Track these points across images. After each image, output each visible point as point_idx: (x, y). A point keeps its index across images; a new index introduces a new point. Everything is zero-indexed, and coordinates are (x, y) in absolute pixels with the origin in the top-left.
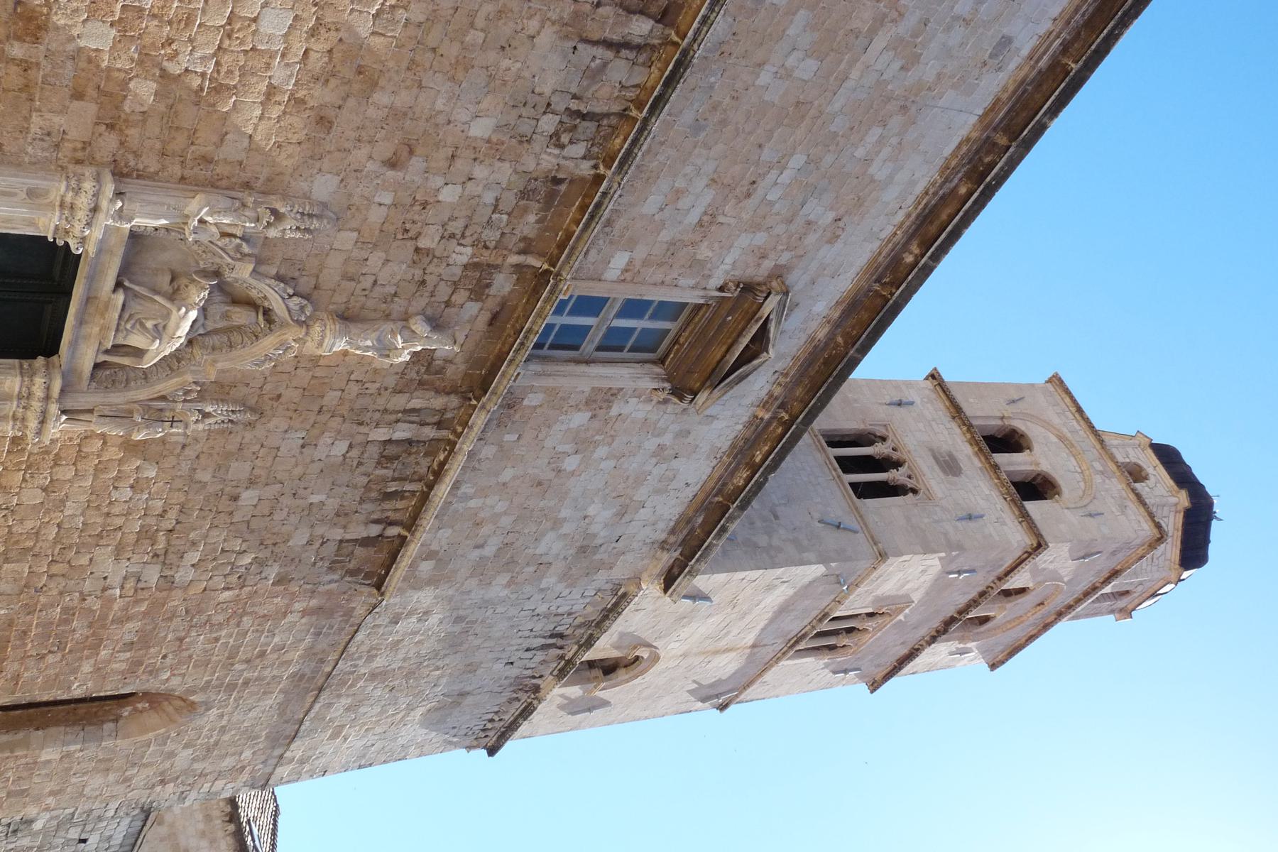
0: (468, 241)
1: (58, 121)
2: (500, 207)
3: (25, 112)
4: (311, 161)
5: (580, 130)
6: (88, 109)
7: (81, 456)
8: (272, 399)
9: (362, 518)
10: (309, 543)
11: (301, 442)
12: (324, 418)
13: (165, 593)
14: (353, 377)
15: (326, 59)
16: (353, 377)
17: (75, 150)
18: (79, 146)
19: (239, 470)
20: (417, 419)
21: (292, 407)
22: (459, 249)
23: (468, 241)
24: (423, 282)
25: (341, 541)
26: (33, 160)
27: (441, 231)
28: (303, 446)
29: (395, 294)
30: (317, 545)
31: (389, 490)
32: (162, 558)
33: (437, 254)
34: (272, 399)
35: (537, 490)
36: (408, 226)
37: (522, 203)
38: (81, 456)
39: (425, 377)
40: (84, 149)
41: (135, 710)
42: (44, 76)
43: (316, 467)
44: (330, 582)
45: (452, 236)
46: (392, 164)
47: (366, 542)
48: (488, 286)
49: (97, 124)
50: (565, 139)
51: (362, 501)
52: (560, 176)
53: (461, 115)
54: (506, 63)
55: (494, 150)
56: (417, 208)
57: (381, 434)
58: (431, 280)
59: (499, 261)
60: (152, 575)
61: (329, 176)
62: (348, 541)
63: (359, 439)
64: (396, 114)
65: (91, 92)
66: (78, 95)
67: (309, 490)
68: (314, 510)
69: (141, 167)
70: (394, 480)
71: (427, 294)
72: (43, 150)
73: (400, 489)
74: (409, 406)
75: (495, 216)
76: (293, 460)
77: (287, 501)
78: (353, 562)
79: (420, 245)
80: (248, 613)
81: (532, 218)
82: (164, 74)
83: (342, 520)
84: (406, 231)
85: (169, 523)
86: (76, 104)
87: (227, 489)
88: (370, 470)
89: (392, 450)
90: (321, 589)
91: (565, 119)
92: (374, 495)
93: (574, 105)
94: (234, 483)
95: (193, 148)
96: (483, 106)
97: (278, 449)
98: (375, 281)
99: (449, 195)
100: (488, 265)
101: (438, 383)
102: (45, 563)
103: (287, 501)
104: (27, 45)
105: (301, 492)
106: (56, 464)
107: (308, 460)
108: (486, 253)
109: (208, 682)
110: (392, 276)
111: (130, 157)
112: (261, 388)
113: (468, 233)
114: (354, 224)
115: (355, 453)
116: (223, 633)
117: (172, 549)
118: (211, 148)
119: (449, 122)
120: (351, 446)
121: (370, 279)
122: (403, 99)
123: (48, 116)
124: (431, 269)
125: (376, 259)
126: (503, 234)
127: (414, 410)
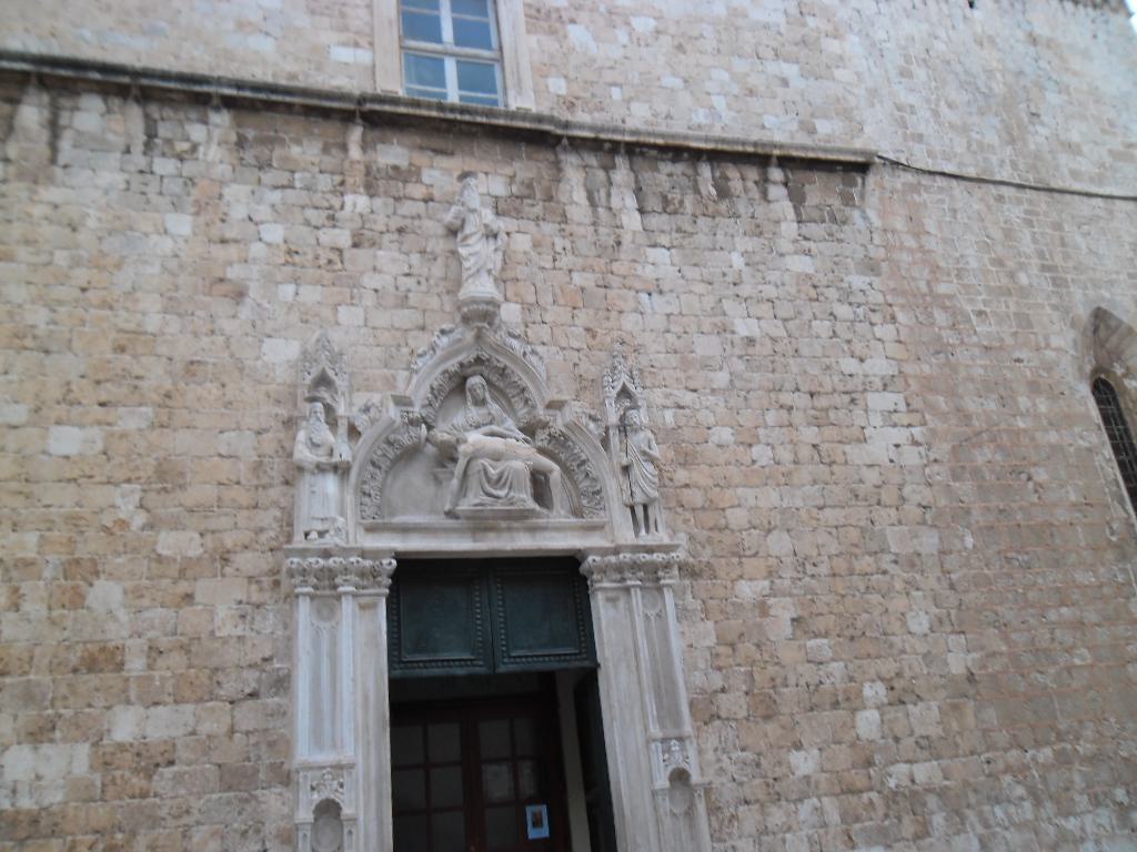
0: (336, 202)
1: (223, 612)
2: (285, 183)
3: (217, 645)
4: (247, 371)
5: (169, 135)
6: (203, 589)
7: (711, 506)
8: (594, 337)
9: (760, 210)
10: (808, 253)
11: (655, 295)
12: (615, 281)
13: (911, 381)
14: (549, 265)
15: (108, 385)
16: (549, 265)
17: (261, 590)
18: (254, 587)
19: (706, 346)
20: (603, 193)
21: (602, 314)
22: (348, 207)
23: (336, 202)
24: (400, 231)
25: (799, 222)
26: (281, 626)
27: (324, 230)
28: (661, 292)
29: (423, 252)
30: (806, 244)
31: (714, 192)
32: (854, 395)
33: (360, 224)
34: (594, 337)
35: (689, 47)
36: (323, 261)
37: (275, 164)
38: (711, 506)
39: (538, 196)
40: (258, 582)
41: (1126, 375)
42: (166, 635)
43: (690, 272)
44: (865, 218)
45: (332, 218)
46: (239, 295)
47: (797, 199)
48: (396, 168)
49: (223, 575)
50: (183, 146)
51: (737, 216)
52: (234, 138)
53: (167, 245)
54: (91, 223)
55: (208, 206)
56: (297, 258)
57: (632, 221)
58: (395, 223)
59: (362, 167)
60: (880, 401)
61: (263, 350)
62: (798, 213)
63: (642, 239)
64: (171, 306)
65: (183, 587)
66: (189, 598)
67: (726, 270)
68: (757, 258)
69: (275, 525)
70: (697, 191)
71: (416, 222)
72: (264, 618)
73: (710, 182)
74: (585, 202)
75: (298, 184)
76: (683, 297)
77: (745, 290)
78: (830, 202)
79: (350, 243)
80: (931, 291)
81: (295, 150)
82: (150, 526)
83: (767, 227)
84: (330, 262)
85: (801, 400)
86: (198, 598)
87: (737, 351)
88: (688, 218)
89: (653, 203)
90: (877, 222)
91: (157, 151)
92: (723, 206)
93: (138, 148)
94: (728, 347)
95: (243, 481)
96: (150, 229)
97: (668, 315)
98: (407, 275)
99: (274, 233)
100: (368, 173)
101: (546, 183)
102: (883, 512)
103: (745, 290)
104: (127, 658)
105: (730, 279)
106: (727, 527)
107: (682, 281)
108: (350, 180)
109: (1055, 307)
110: (394, 260)
111: (263, 538)
112: (578, 350)
113: (326, 204)
114: (326, 312)
115: (664, 239)
116: (968, 308)
117: (840, 387)
118: (241, 466)
119: (176, 256)
120: (654, 246)
121: (403, 281)
122: (151, 305)
123: (218, 621)
124: (380, 227)
125: (371, 281)
126: (321, 172)
127: (591, 198)
